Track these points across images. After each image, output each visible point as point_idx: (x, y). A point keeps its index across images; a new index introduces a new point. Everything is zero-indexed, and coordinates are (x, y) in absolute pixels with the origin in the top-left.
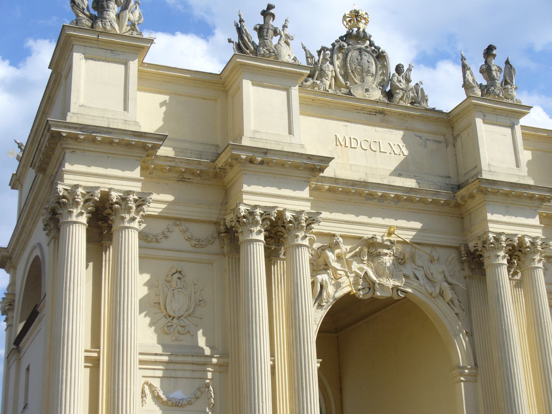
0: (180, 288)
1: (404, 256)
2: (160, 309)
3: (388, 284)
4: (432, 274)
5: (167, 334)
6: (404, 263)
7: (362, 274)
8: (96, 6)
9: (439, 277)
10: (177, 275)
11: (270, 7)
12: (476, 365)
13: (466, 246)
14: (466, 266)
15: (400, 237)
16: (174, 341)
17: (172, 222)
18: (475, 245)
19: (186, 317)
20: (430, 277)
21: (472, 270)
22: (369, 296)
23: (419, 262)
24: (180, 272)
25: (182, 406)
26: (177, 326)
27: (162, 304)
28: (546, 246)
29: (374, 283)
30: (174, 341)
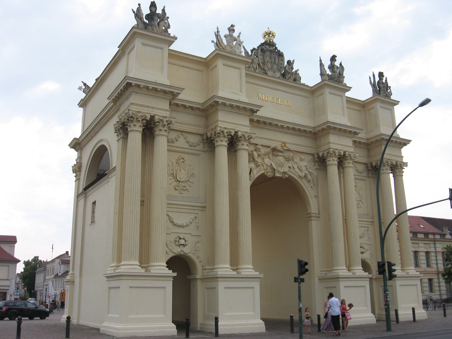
0: (183, 167)
1: (289, 157)
4: (301, 167)
7: (269, 164)
8: (147, 18)
9: (304, 168)
10: (182, 160)
13: (318, 154)
14: (317, 164)
15: (287, 147)
16: (179, 194)
17: (179, 134)
18: (322, 154)
19: (186, 182)
21: (319, 165)
24: (183, 159)
25: (184, 227)
26: (181, 186)
28: (355, 157)
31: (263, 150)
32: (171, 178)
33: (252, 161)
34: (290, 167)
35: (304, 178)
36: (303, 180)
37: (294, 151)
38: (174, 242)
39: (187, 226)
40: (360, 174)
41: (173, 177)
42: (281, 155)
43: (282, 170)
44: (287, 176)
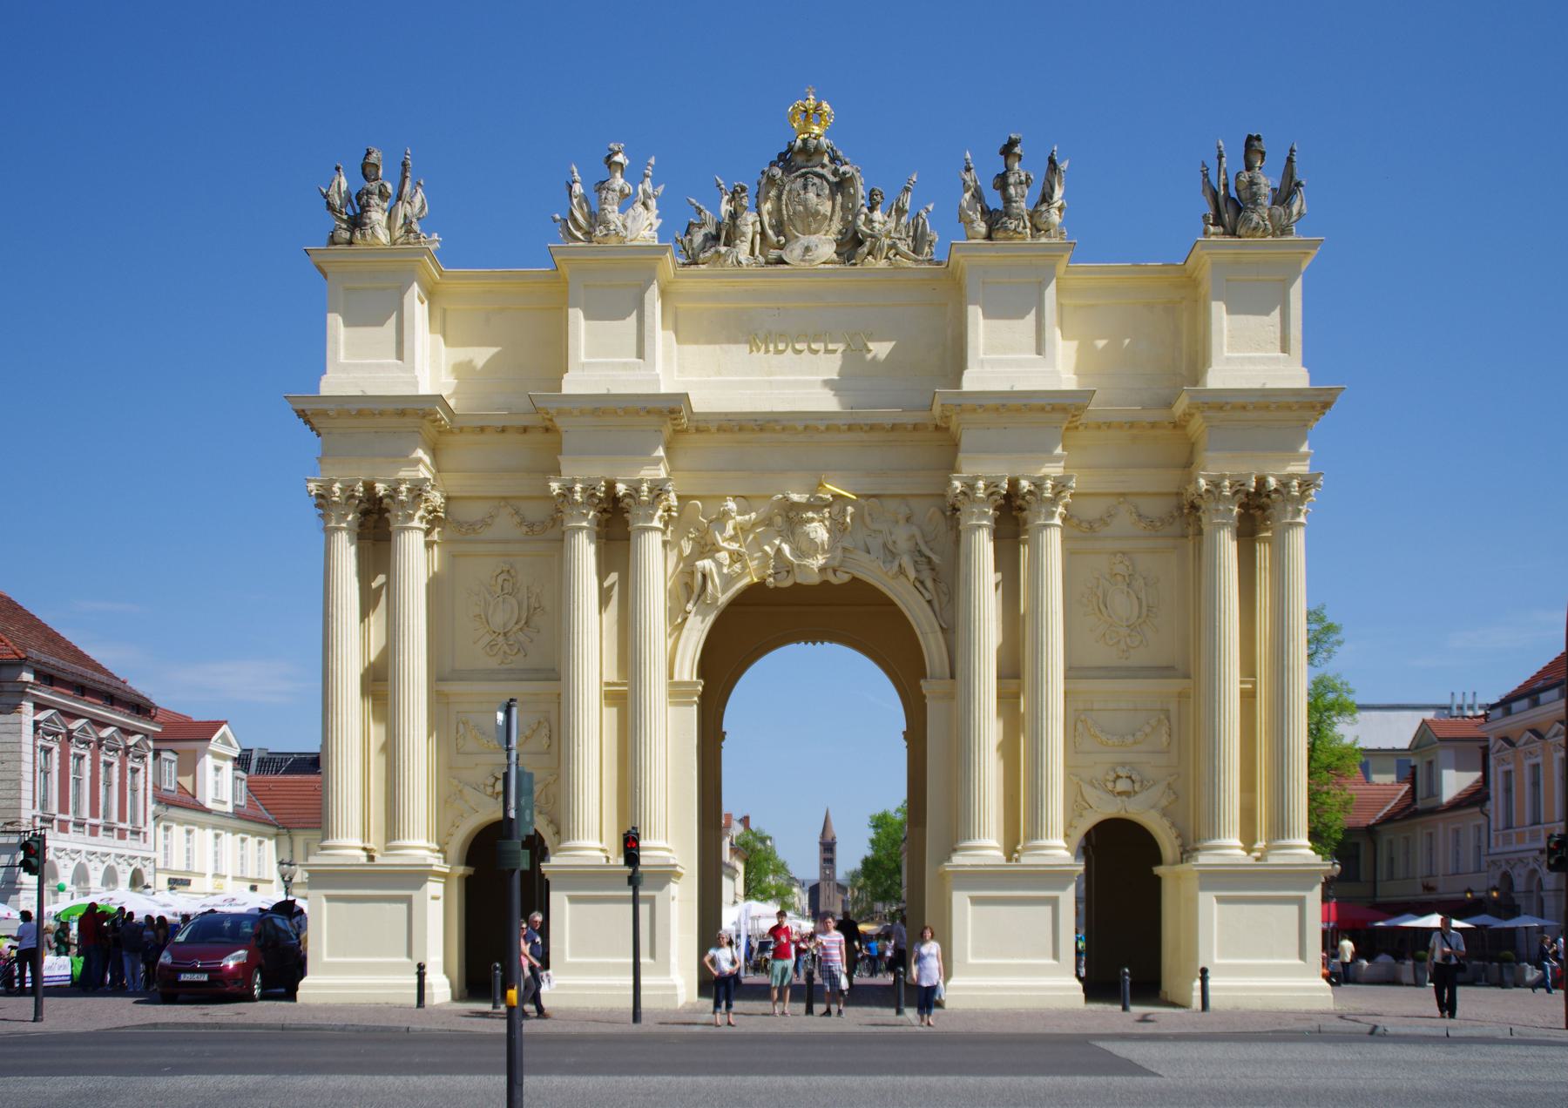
0: (507, 594)
3: (813, 565)
5: (491, 656)
16: (499, 664)
20: (891, 547)
22: (787, 583)
27: (483, 616)
29: (792, 564)
30: (499, 664)
38: (482, 786)
44: (846, 578)
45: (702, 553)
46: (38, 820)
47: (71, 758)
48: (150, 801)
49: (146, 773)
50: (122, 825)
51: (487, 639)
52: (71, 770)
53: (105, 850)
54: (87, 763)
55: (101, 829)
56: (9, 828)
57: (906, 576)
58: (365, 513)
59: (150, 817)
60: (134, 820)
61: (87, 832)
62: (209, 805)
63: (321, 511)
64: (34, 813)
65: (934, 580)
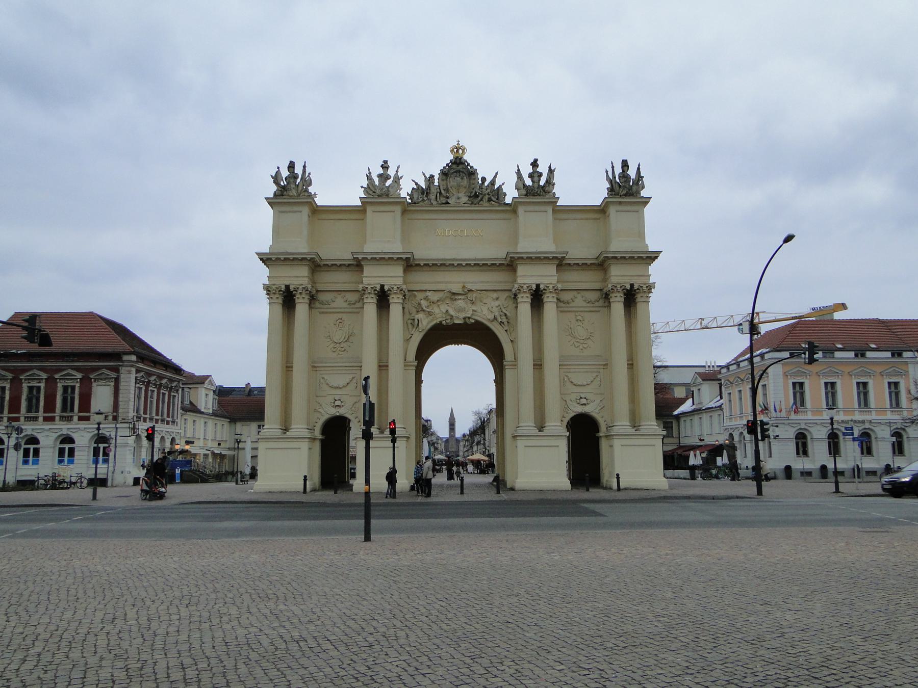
2: (330, 339)
5: (334, 352)
6: (473, 302)
11: (386, 162)
12: (515, 359)
20: (491, 309)
23: (485, 301)
24: (341, 319)
25: (340, 388)
31: (434, 297)
32: (329, 340)
33: (421, 311)
34: (473, 311)
35: (495, 321)
36: (493, 322)
37: (479, 290)
39: (344, 387)
40: (591, 305)
41: (330, 339)
42: (460, 299)
43: (462, 315)
44: (473, 321)
45: (417, 312)
46: (135, 417)
47: (149, 392)
48: (179, 408)
49: (178, 398)
50: (168, 419)
51: (332, 345)
52: (149, 397)
53: (161, 429)
54: (155, 393)
55: (160, 421)
56: (123, 421)
57: (497, 320)
58: (285, 297)
59: (179, 416)
60: (173, 417)
61: (154, 422)
62: (203, 410)
63: (268, 296)
64: (134, 414)
65: (508, 322)
